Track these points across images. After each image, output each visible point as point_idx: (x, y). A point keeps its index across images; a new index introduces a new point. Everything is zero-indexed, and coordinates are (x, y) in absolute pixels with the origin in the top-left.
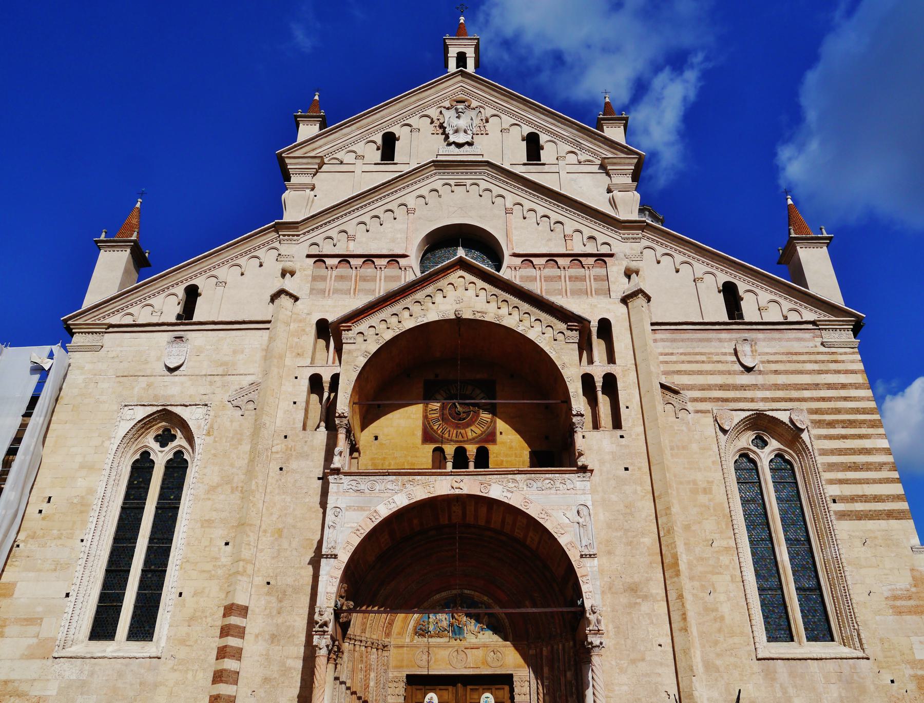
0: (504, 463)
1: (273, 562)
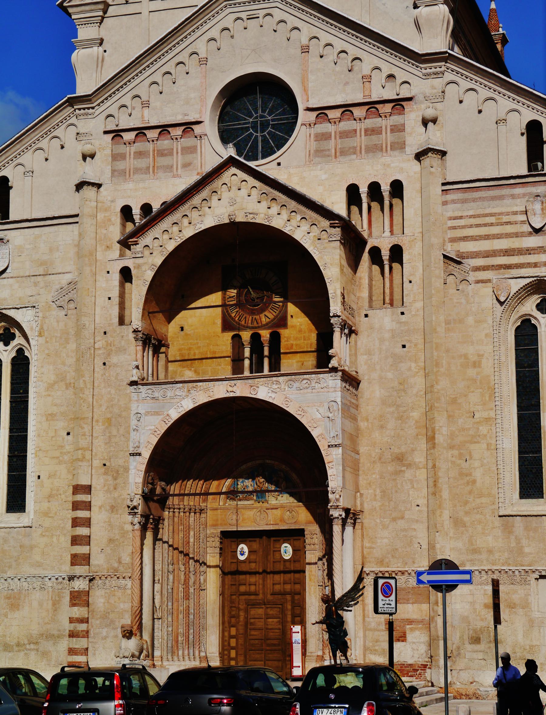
0: (294, 347)
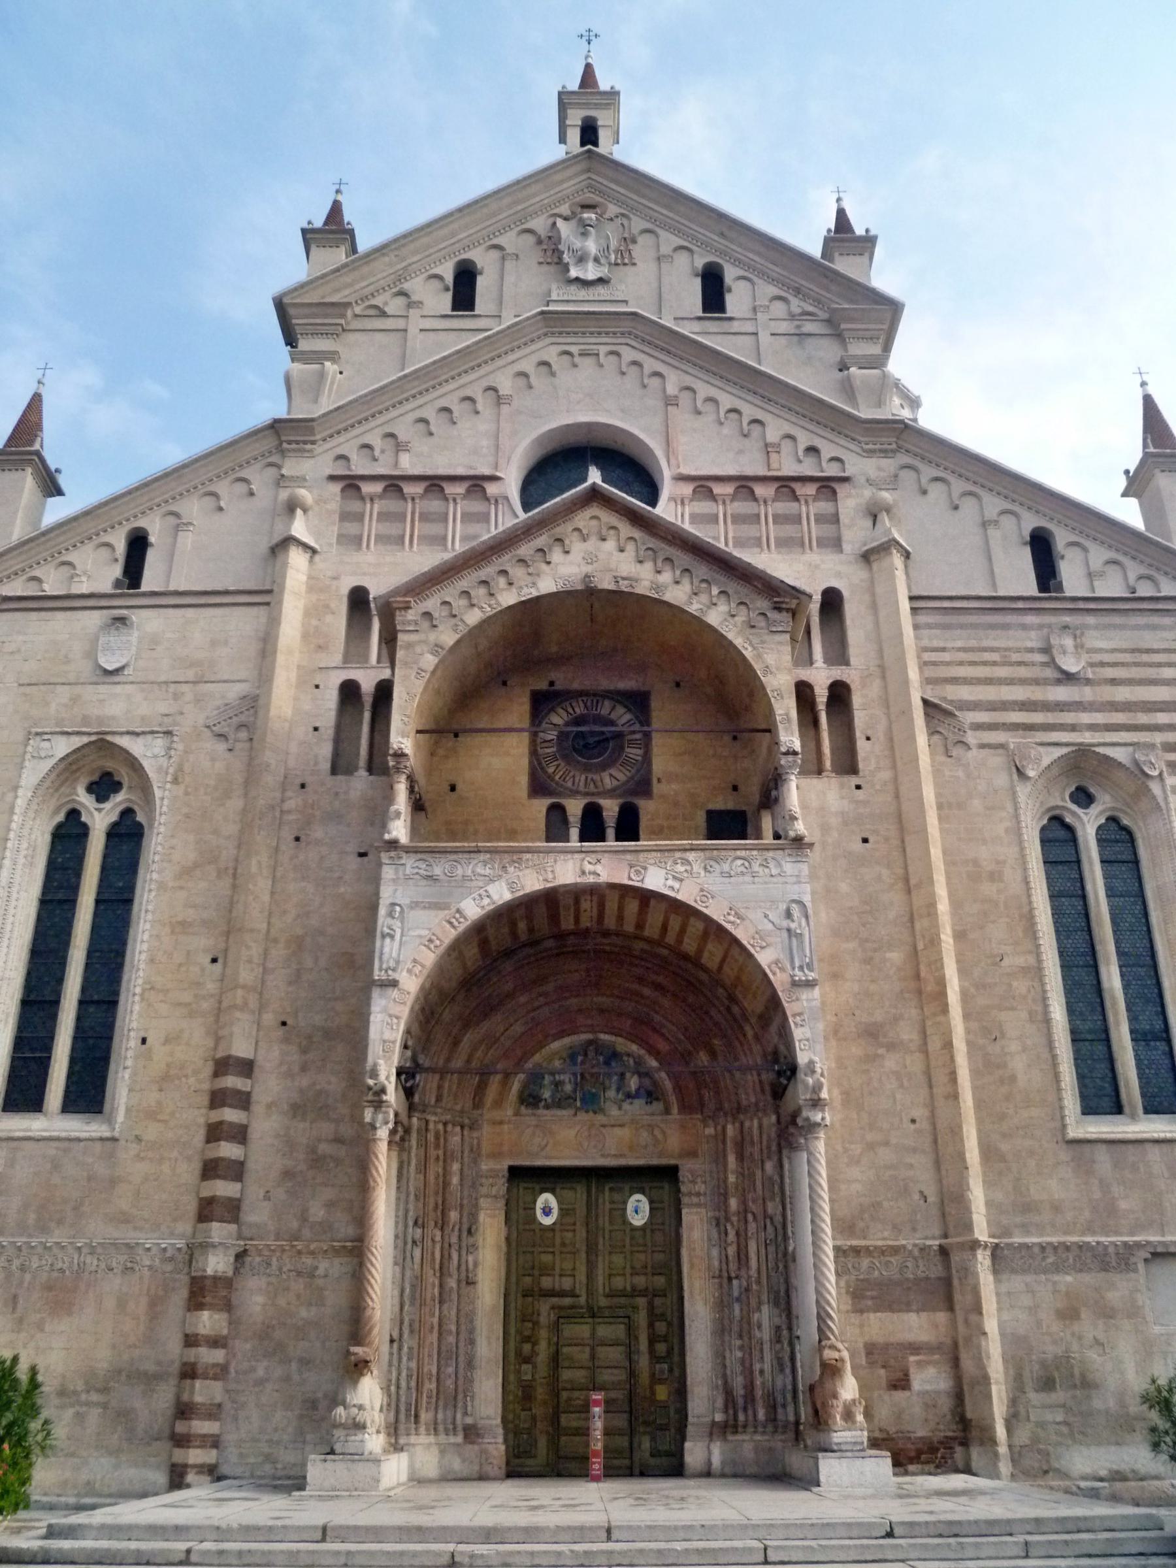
1: (290, 989)
